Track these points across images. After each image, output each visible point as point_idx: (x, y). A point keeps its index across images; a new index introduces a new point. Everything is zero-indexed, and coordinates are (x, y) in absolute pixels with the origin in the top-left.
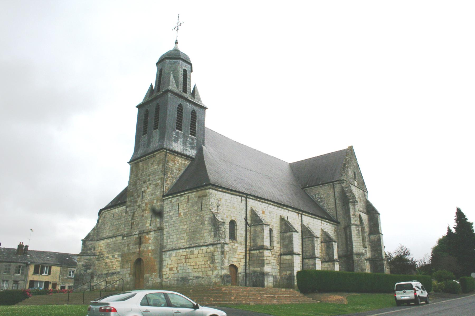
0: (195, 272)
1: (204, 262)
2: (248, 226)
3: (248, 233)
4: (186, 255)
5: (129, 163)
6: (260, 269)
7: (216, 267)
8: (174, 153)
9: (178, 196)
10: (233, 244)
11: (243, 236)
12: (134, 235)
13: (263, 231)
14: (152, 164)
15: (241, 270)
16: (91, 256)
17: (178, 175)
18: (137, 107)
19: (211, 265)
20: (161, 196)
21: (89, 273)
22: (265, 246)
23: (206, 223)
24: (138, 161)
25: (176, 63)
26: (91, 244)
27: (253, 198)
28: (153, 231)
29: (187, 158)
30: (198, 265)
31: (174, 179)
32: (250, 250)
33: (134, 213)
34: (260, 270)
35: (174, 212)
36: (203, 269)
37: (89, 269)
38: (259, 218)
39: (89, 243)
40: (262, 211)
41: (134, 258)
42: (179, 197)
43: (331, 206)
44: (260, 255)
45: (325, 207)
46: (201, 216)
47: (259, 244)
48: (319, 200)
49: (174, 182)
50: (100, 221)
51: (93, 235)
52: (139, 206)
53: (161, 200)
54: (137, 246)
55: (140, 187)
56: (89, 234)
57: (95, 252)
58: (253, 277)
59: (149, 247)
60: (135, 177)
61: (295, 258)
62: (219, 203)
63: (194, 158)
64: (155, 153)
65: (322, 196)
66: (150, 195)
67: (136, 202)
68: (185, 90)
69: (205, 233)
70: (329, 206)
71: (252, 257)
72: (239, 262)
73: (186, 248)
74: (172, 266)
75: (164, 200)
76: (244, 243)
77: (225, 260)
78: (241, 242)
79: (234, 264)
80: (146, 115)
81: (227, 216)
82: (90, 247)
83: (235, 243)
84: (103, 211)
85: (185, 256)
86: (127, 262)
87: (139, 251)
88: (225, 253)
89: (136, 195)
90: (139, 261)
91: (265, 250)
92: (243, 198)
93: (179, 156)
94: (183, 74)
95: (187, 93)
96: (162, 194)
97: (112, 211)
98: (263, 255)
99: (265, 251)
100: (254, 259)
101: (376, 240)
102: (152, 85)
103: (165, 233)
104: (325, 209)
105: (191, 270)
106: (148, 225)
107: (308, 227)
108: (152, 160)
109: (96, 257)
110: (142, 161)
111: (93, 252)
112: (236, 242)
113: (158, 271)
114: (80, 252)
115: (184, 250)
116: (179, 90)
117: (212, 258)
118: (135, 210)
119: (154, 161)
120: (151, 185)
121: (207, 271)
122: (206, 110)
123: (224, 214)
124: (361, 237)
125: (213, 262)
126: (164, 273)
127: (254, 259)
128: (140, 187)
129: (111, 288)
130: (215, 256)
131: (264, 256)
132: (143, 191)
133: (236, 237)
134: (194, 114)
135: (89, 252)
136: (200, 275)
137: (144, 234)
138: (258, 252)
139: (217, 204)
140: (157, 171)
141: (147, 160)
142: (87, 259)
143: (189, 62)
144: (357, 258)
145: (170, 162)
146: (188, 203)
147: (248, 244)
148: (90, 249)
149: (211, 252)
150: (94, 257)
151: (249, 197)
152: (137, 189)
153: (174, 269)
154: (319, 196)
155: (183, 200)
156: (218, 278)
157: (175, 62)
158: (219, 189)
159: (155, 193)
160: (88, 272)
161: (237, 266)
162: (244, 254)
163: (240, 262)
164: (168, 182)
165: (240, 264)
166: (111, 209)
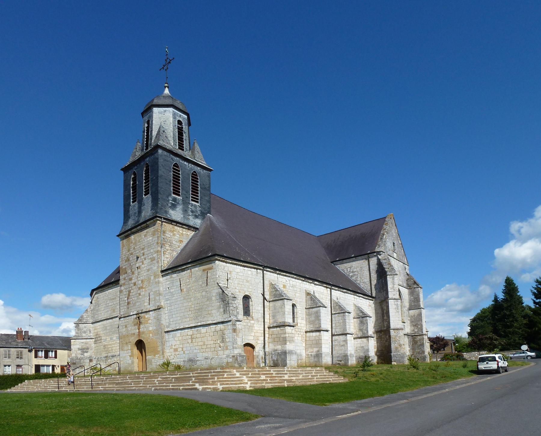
10: (248, 321)
19: (221, 345)
23: (214, 298)
33: (130, 292)
36: (213, 349)
40: (283, 285)
43: (365, 280)
45: (359, 281)
48: (351, 274)
52: (135, 284)
65: (355, 270)
69: (213, 310)
70: (362, 280)
77: (237, 338)
81: (240, 290)
85: (191, 335)
88: (238, 332)
89: (130, 271)
98: (284, 332)
101: (416, 315)
104: (358, 284)
106: (146, 304)
107: (339, 302)
117: (222, 337)
121: (217, 351)
123: (236, 288)
124: (400, 311)
133: (252, 313)
144: (395, 333)
152: (130, 264)
154: (351, 270)
156: (231, 358)
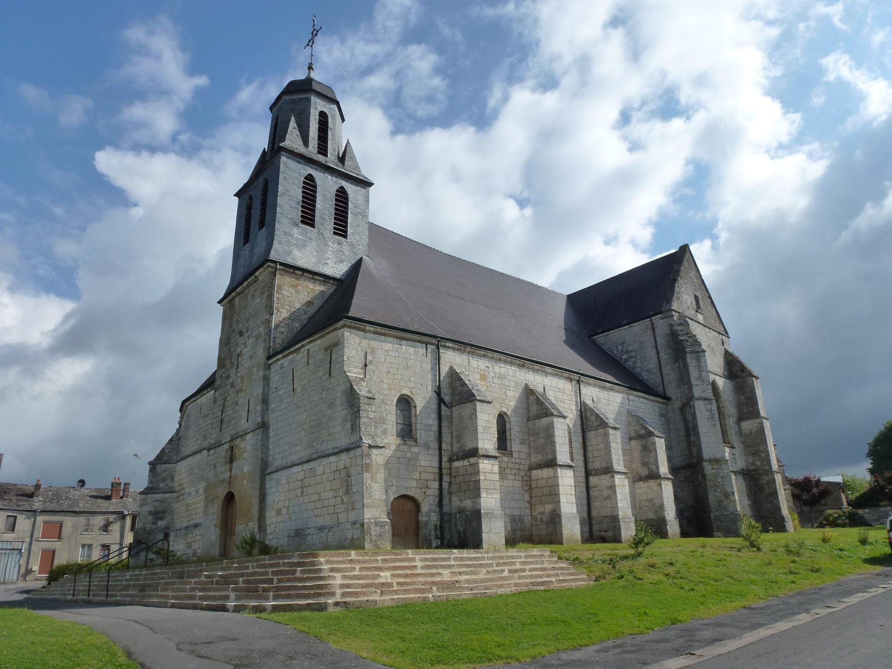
0: (318, 516)
1: (332, 491)
2: (443, 407)
3: (444, 424)
4: (303, 480)
5: (219, 302)
6: (472, 501)
7: (353, 504)
8: (294, 270)
9: (291, 353)
10: (406, 447)
11: (432, 431)
12: (224, 443)
13: (476, 417)
14: (253, 296)
15: (428, 506)
16: (164, 493)
17: (306, 314)
18: (236, 195)
19: (346, 500)
20: (265, 358)
21: (160, 528)
22: (482, 449)
23: (338, 402)
24: (233, 297)
25: (304, 100)
26: (165, 471)
27: (456, 346)
28: (250, 432)
29: (326, 280)
30: (323, 500)
31: (297, 322)
32: (451, 460)
33: (225, 399)
34: (472, 506)
35: (285, 388)
36: (331, 510)
37: (162, 519)
38: (468, 386)
39: (162, 469)
40: (480, 374)
41: (222, 492)
42: (294, 355)
43: (650, 366)
44: (470, 470)
45: (639, 369)
46: (330, 389)
47: (469, 446)
48: (624, 357)
49: (295, 329)
50: (183, 424)
51: (170, 452)
52: (233, 386)
53: (264, 367)
54: (228, 466)
55: (234, 348)
56: (163, 451)
57: (174, 484)
58: (459, 522)
59: (244, 466)
60: (228, 328)
61: (562, 474)
62: (369, 357)
63: (344, 279)
64: (257, 274)
65: (630, 348)
66: (249, 358)
67: (228, 377)
68: (323, 149)
69: (336, 426)
70: (645, 366)
71: (455, 477)
72: (422, 488)
73: (302, 463)
74: (280, 505)
75: (270, 365)
76: (434, 445)
77: (373, 484)
78: (426, 444)
79: (411, 493)
80: (249, 208)
81: (391, 386)
82: (164, 475)
83: (410, 446)
84: (187, 404)
85: (302, 480)
86: (212, 501)
87: (230, 476)
88: (374, 470)
89: (228, 363)
90: (230, 498)
91: (479, 458)
92: (430, 347)
93: (306, 277)
94: (319, 120)
95: (329, 155)
96: (266, 355)
97: (198, 401)
98: (476, 471)
99: (480, 461)
100: (459, 479)
101: (754, 430)
102: (264, 148)
103: (271, 435)
104: (638, 374)
105: (310, 511)
106: (243, 421)
107: (596, 408)
108: (253, 289)
109: (174, 494)
110: (238, 295)
111: (170, 485)
112: (413, 443)
113: (256, 517)
114: (146, 486)
115: (300, 468)
116: (312, 150)
117: (347, 481)
118: (227, 394)
119: (255, 290)
120: (250, 339)
121: (337, 513)
122: (371, 189)
123: (382, 382)
124: (718, 423)
125: (349, 491)
126: (268, 521)
127: (459, 479)
128: (234, 348)
129: (191, 555)
130: (352, 478)
131: (478, 473)
132: (238, 354)
133: (414, 432)
134: (342, 197)
135: (162, 485)
136: (327, 524)
137: (238, 440)
138: (466, 462)
139: (363, 360)
140: (259, 308)
141: (247, 290)
142: (157, 501)
143: (335, 99)
144: (713, 469)
145: (286, 288)
146: (308, 364)
147: (444, 446)
148: (164, 480)
149: (345, 468)
150: (171, 495)
151: (444, 344)
152: (230, 350)
153: (284, 511)
154: (624, 349)
155: (300, 360)
156: (357, 529)
157: (301, 99)
158: (368, 328)
159: (255, 353)
160: (159, 526)
161: (416, 497)
162: (437, 470)
163: (427, 490)
164: (281, 328)
165: (425, 493)
166: (197, 399)
